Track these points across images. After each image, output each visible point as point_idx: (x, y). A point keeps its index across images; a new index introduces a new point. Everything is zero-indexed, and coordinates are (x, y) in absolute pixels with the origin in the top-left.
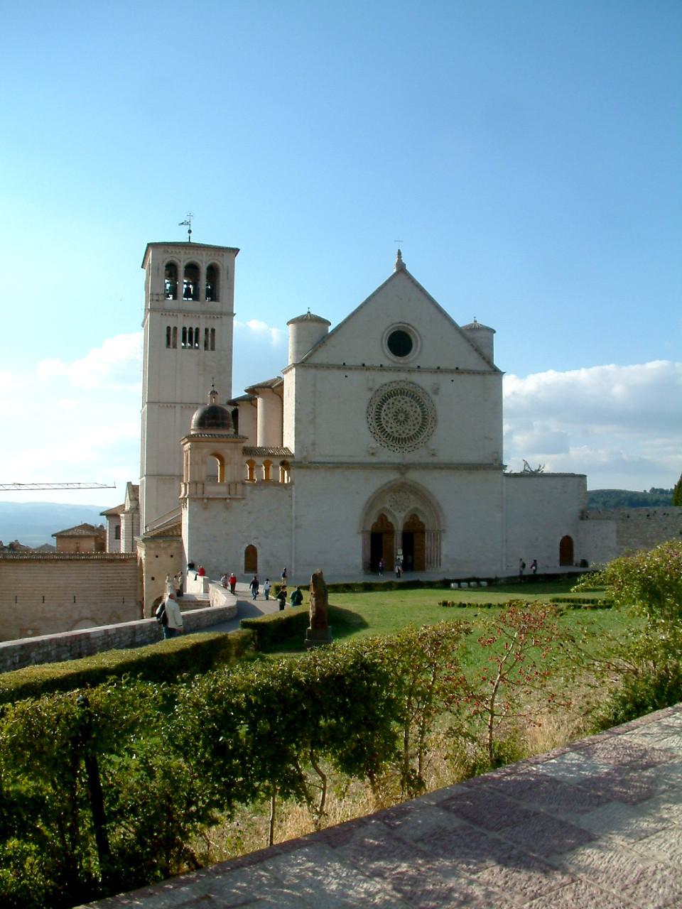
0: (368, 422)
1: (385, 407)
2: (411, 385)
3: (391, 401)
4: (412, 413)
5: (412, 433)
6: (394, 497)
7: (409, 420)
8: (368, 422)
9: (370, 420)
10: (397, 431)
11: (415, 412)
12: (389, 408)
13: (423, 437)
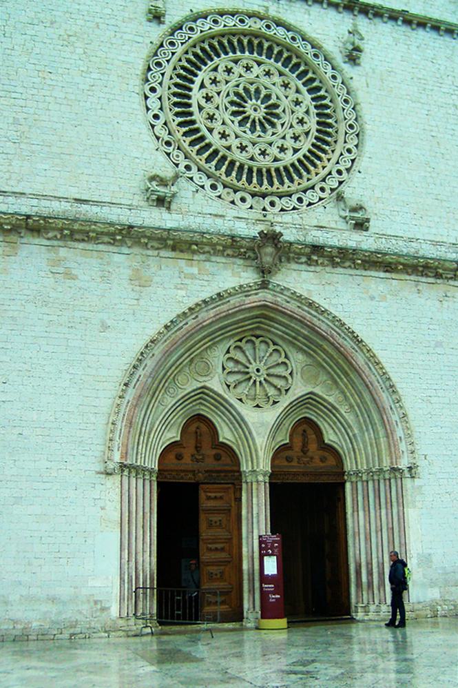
0: (148, 109)
1: (203, 75)
2: (281, 30)
3: (223, 61)
4: (285, 103)
5: (289, 158)
6: (239, 356)
7: (278, 122)
8: (148, 109)
9: (153, 103)
10: (242, 148)
11: (297, 103)
12: (214, 81)
13: (323, 173)
